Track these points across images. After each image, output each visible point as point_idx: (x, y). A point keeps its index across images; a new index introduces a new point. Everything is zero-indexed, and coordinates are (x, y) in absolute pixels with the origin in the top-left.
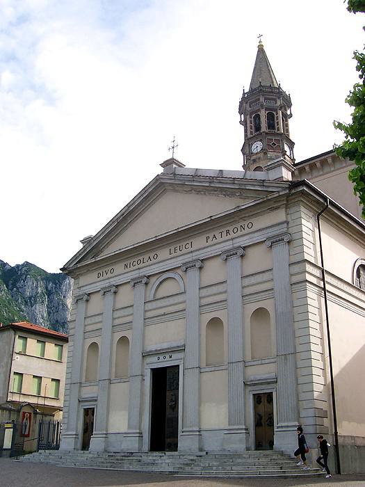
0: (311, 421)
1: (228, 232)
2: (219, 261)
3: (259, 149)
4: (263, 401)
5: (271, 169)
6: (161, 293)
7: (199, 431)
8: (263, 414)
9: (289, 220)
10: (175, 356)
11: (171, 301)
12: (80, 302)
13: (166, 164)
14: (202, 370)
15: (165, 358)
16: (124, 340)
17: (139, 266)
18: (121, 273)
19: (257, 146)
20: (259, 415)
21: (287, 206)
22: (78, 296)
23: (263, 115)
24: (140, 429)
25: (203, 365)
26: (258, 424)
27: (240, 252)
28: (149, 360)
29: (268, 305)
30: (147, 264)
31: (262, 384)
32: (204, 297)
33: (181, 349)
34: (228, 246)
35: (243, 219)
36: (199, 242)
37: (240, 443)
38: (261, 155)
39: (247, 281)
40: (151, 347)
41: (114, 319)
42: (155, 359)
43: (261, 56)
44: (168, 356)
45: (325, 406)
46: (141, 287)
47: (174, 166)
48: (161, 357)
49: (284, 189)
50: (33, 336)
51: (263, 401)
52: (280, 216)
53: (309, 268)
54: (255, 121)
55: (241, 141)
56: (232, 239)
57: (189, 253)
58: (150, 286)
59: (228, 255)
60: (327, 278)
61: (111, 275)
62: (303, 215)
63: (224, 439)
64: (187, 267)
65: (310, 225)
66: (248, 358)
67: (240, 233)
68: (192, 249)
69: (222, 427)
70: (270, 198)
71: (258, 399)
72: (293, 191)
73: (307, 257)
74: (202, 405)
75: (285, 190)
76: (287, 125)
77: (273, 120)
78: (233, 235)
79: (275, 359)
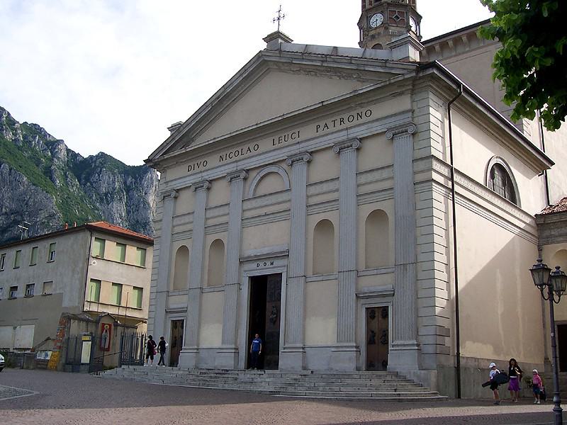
0: (431, 340)
2: (330, 154)
3: (379, 23)
4: (377, 315)
5: (395, 47)
6: (263, 189)
7: (303, 348)
8: (376, 331)
9: (415, 108)
10: (277, 263)
12: (167, 199)
13: (270, 39)
14: (309, 280)
15: (265, 264)
16: (218, 244)
17: (237, 158)
18: (216, 166)
19: (377, 20)
20: (373, 332)
21: (413, 92)
22: (165, 193)
24: (236, 343)
25: (310, 273)
26: (371, 341)
27: (356, 144)
28: (247, 266)
29: (386, 206)
30: (246, 156)
32: (311, 196)
33: (285, 255)
34: (342, 136)
35: (361, 105)
36: (308, 132)
37: (349, 362)
38: (382, 30)
39: (363, 179)
40: (250, 252)
41: (207, 219)
42: (254, 265)
44: (268, 263)
45: (446, 323)
46: (239, 183)
47: (280, 41)
48: (262, 264)
49: (411, 71)
50: (111, 238)
51: (377, 315)
52: (404, 103)
53: (436, 166)
55: (359, 12)
56: (347, 129)
58: (249, 181)
59: (341, 148)
60: (457, 178)
62: (431, 103)
63: (331, 356)
64: (293, 160)
65: (439, 115)
66: (362, 266)
67: (355, 122)
68: (299, 140)
69: (329, 344)
70: (392, 81)
71: (371, 313)
72: (421, 75)
73: (434, 152)
74: (307, 320)
75: (411, 72)
78: (347, 124)
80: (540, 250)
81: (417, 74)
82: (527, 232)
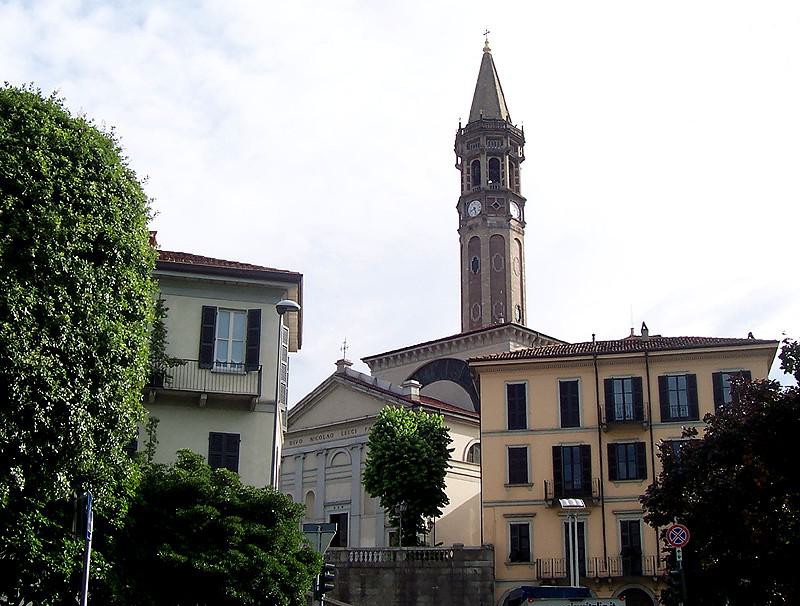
13: (340, 363)
19: (475, 207)
23: (484, 161)
28: (328, 509)
38: (479, 221)
43: (487, 61)
54: (473, 169)
76: (517, 174)
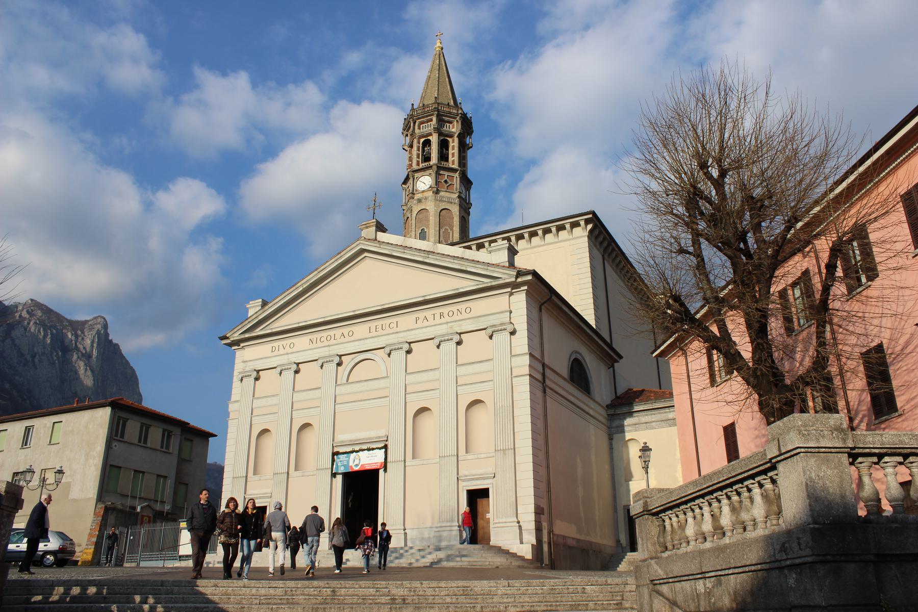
1: (441, 315)
3: (426, 187)
6: (356, 375)
11: (371, 385)
17: (330, 343)
30: (339, 341)
31: (477, 479)
36: (406, 320)
54: (423, 151)
57: (393, 333)
61: (290, 350)
68: (398, 329)
77: (447, 149)
79: (494, 454)
80: (611, 439)
81: (516, 279)
82: (602, 423)
